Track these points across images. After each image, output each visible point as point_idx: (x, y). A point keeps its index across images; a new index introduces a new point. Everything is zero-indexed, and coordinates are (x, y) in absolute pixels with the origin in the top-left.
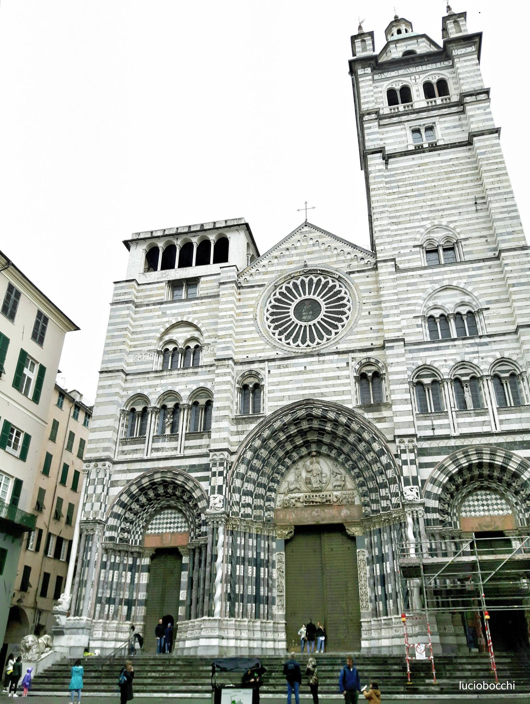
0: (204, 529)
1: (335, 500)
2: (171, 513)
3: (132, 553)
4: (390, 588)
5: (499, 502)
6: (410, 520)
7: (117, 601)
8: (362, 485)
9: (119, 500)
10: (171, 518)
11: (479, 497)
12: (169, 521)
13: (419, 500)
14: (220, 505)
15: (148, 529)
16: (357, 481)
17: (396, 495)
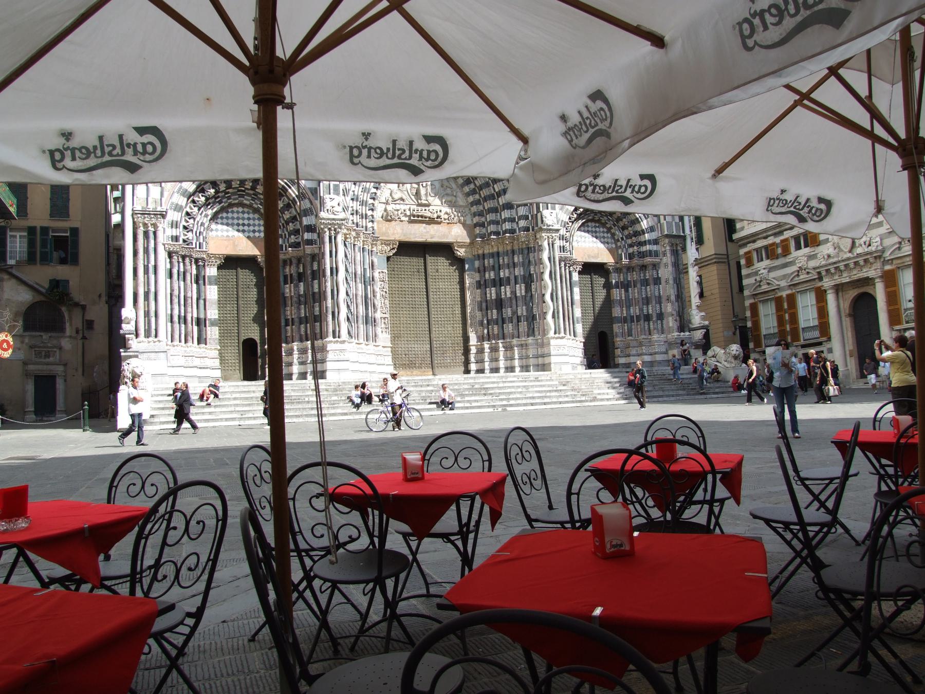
0: (307, 236)
1: (446, 216)
2: (243, 212)
3: (197, 261)
4: (508, 312)
5: (606, 235)
6: (545, 244)
7: (189, 319)
8: (477, 203)
9: (181, 187)
10: (243, 219)
11: (590, 229)
12: (241, 222)
13: (556, 227)
14: (340, 209)
15: (212, 230)
16: (471, 199)
17: (526, 218)
